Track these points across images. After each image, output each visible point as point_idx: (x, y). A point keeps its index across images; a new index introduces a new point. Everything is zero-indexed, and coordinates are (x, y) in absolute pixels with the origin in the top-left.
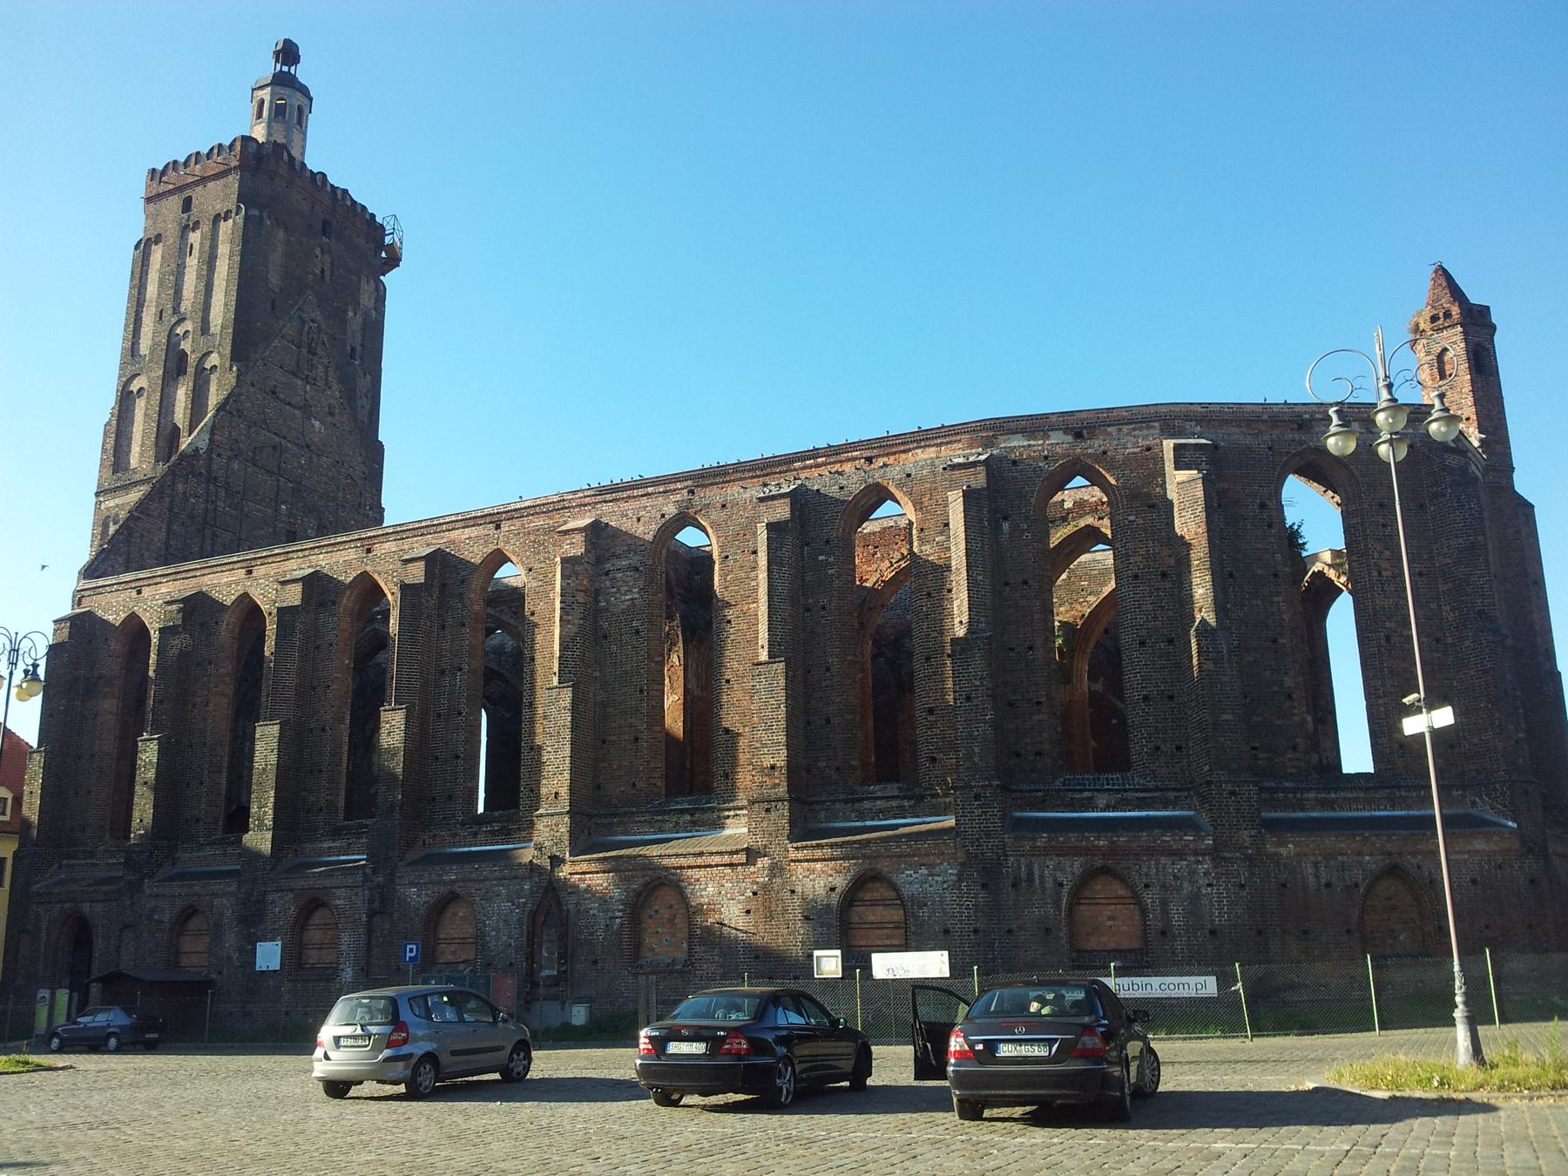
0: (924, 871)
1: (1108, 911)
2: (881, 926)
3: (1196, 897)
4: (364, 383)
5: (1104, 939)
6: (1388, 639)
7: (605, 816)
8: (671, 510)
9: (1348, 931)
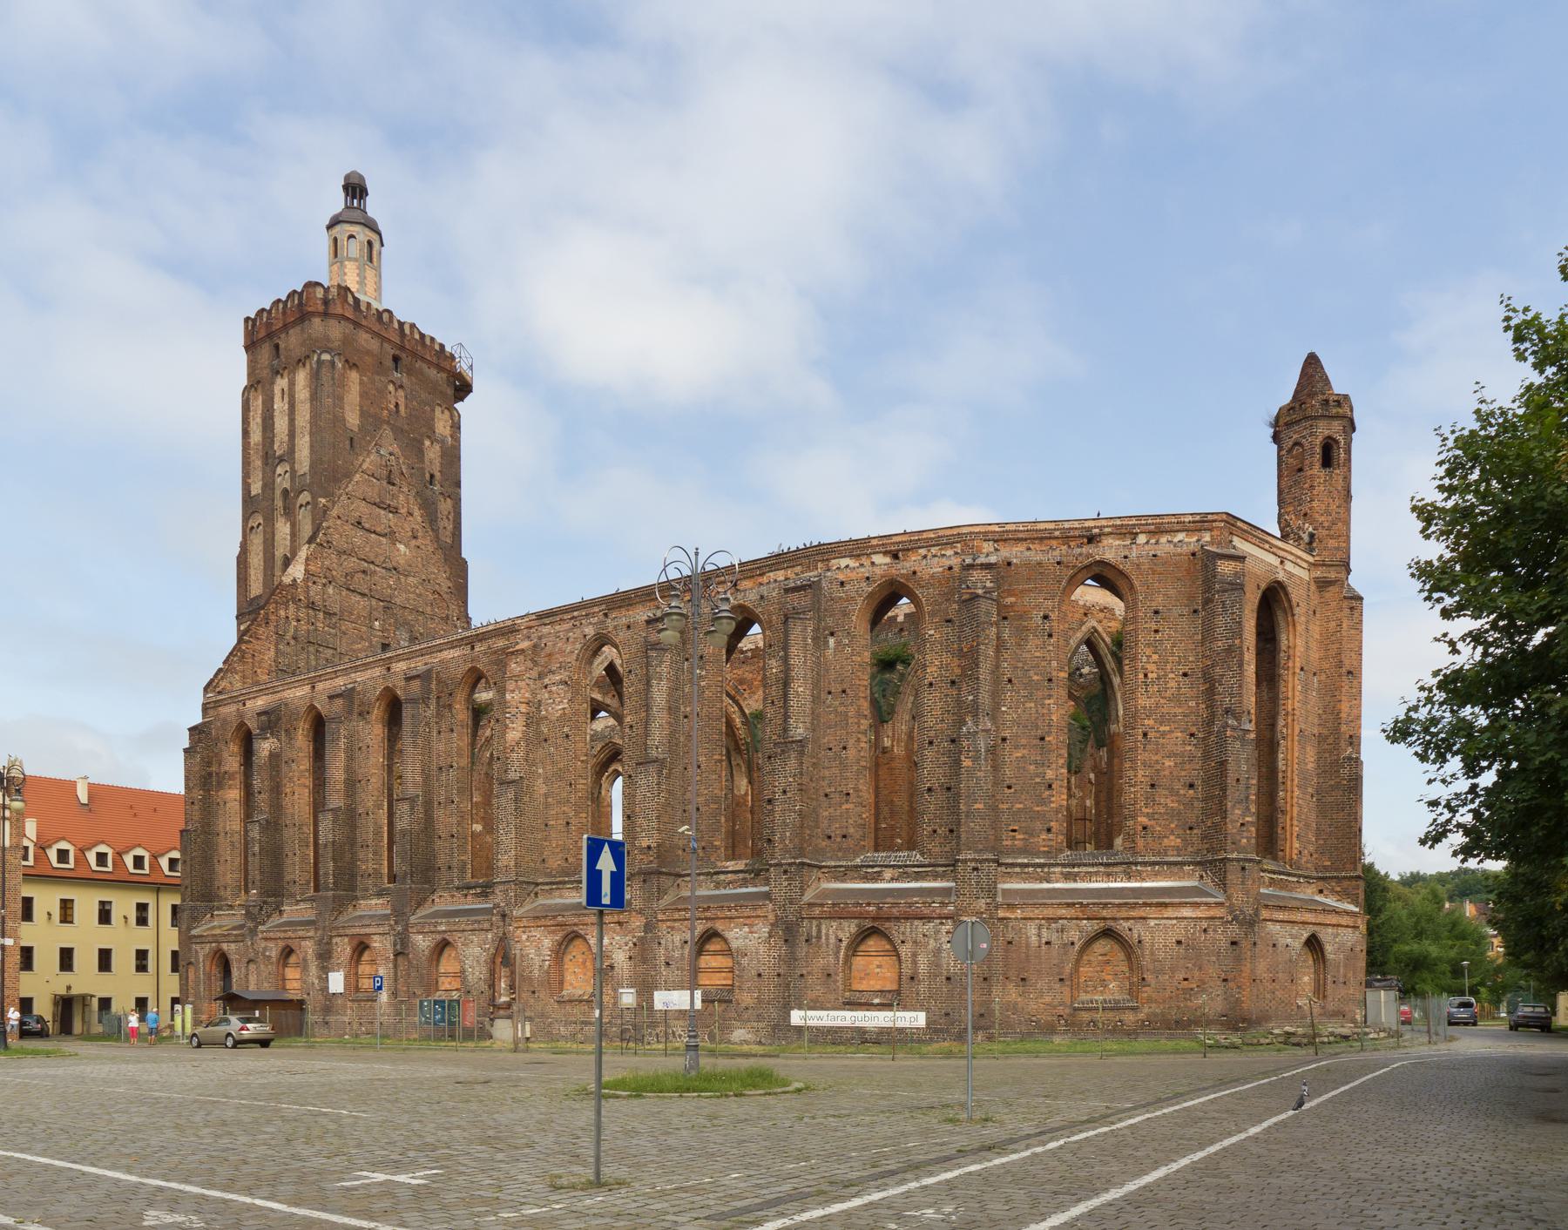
0: (746, 929)
2: (719, 970)
6: (1145, 735)
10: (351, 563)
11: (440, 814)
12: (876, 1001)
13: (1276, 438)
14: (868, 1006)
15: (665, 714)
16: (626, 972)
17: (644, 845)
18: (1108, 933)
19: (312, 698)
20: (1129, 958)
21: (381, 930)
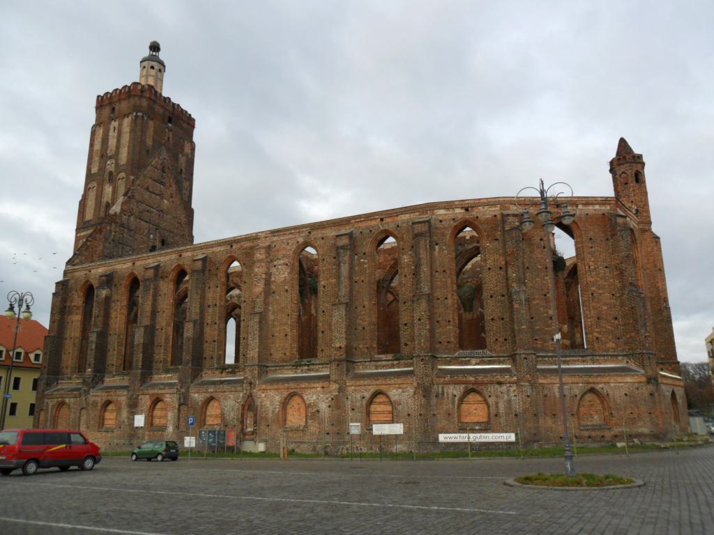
0: (400, 390)
1: (474, 407)
2: (383, 412)
3: (509, 401)
4: (186, 184)
5: (472, 418)
6: (592, 294)
7: (273, 367)
8: (301, 240)
9: (573, 415)
10: (143, 207)
11: (207, 330)
12: (477, 428)
13: (611, 171)
14: (473, 431)
15: (347, 280)
16: (327, 416)
17: (338, 345)
18: (592, 390)
19: (132, 269)
20: (602, 403)
21: (171, 391)
